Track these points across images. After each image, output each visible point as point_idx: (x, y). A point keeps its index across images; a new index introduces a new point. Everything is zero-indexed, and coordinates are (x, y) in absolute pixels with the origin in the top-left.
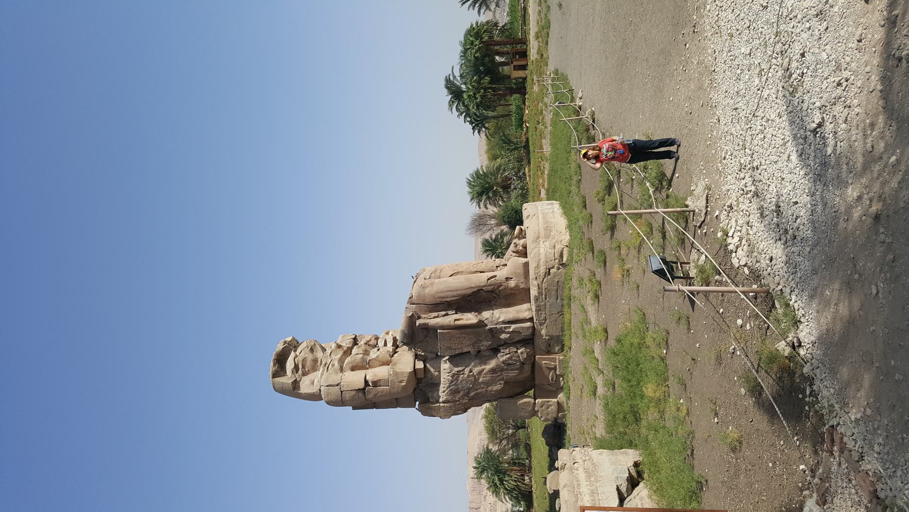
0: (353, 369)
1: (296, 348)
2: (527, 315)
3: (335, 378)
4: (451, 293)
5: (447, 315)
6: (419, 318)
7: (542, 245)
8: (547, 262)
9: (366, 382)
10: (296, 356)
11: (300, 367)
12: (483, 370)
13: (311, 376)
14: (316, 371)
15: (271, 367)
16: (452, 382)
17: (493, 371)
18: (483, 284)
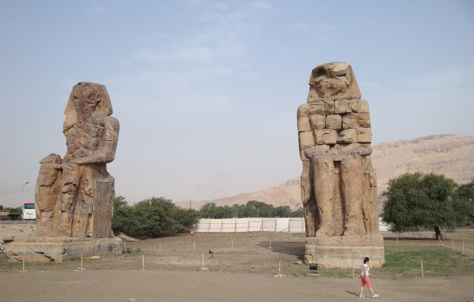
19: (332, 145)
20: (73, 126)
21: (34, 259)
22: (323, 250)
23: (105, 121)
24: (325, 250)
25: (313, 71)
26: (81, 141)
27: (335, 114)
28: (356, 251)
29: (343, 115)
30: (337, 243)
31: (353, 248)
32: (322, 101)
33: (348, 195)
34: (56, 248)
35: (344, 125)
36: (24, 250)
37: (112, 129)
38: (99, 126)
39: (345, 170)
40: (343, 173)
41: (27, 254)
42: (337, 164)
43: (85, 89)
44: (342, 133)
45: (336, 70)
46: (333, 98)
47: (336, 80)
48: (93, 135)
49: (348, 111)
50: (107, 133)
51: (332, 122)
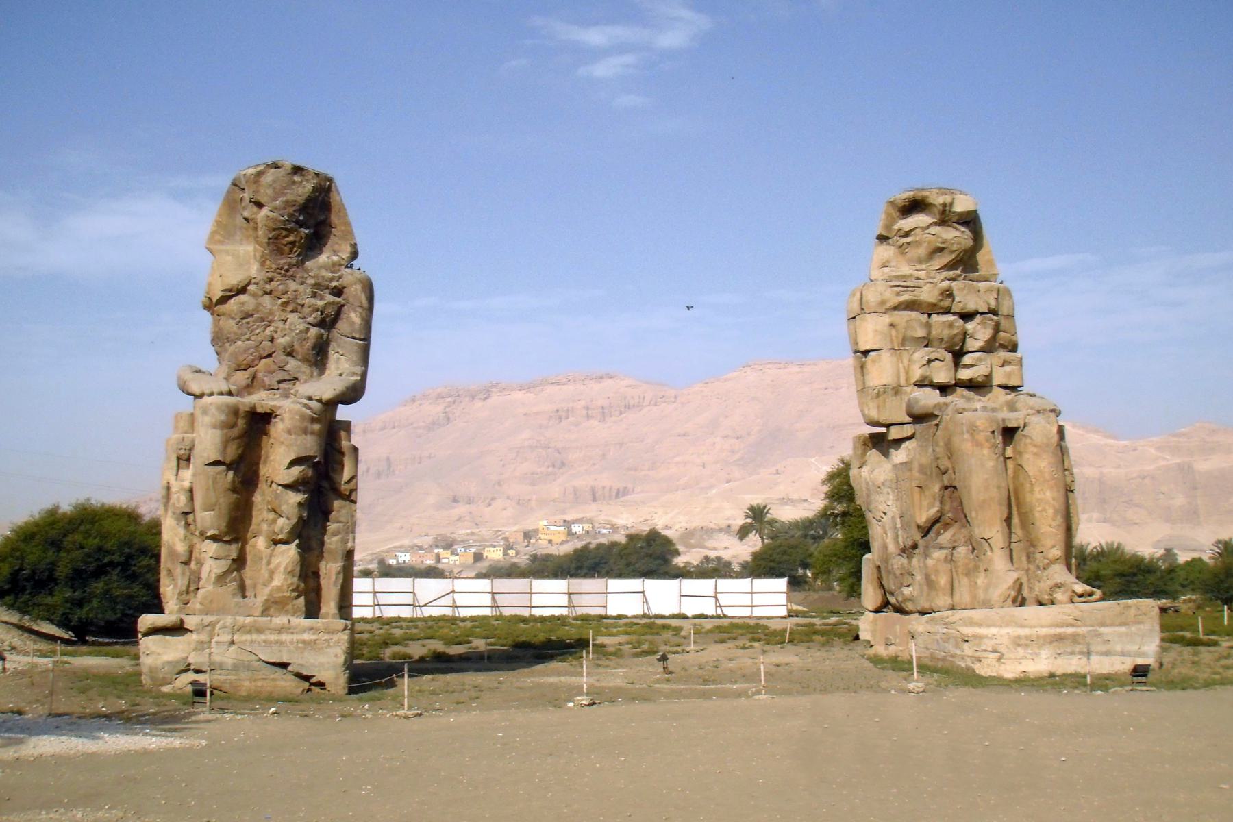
1: (943, 222)
7: (1004, 631)
8: (976, 637)
15: (902, 194)
20: (243, 290)
21: (259, 684)
22: (1038, 637)
23: (344, 282)
26: (275, 336)
27: (948, 311)
28: (1109, 638)
29: (967, 316)
31: (1102, 630)
33: (1044, 510)
34: (332, 651)
35: (972, 344)
36: (227, 657)
37: (365, 303)
38: (330, 298)
39: (1035, 450)
40: (1026, 456)
41: (236, 668)
42: (1009, 433)
43: (294, 182)
44: (967, 359)
48: (309, 319)
50: (353, 315)
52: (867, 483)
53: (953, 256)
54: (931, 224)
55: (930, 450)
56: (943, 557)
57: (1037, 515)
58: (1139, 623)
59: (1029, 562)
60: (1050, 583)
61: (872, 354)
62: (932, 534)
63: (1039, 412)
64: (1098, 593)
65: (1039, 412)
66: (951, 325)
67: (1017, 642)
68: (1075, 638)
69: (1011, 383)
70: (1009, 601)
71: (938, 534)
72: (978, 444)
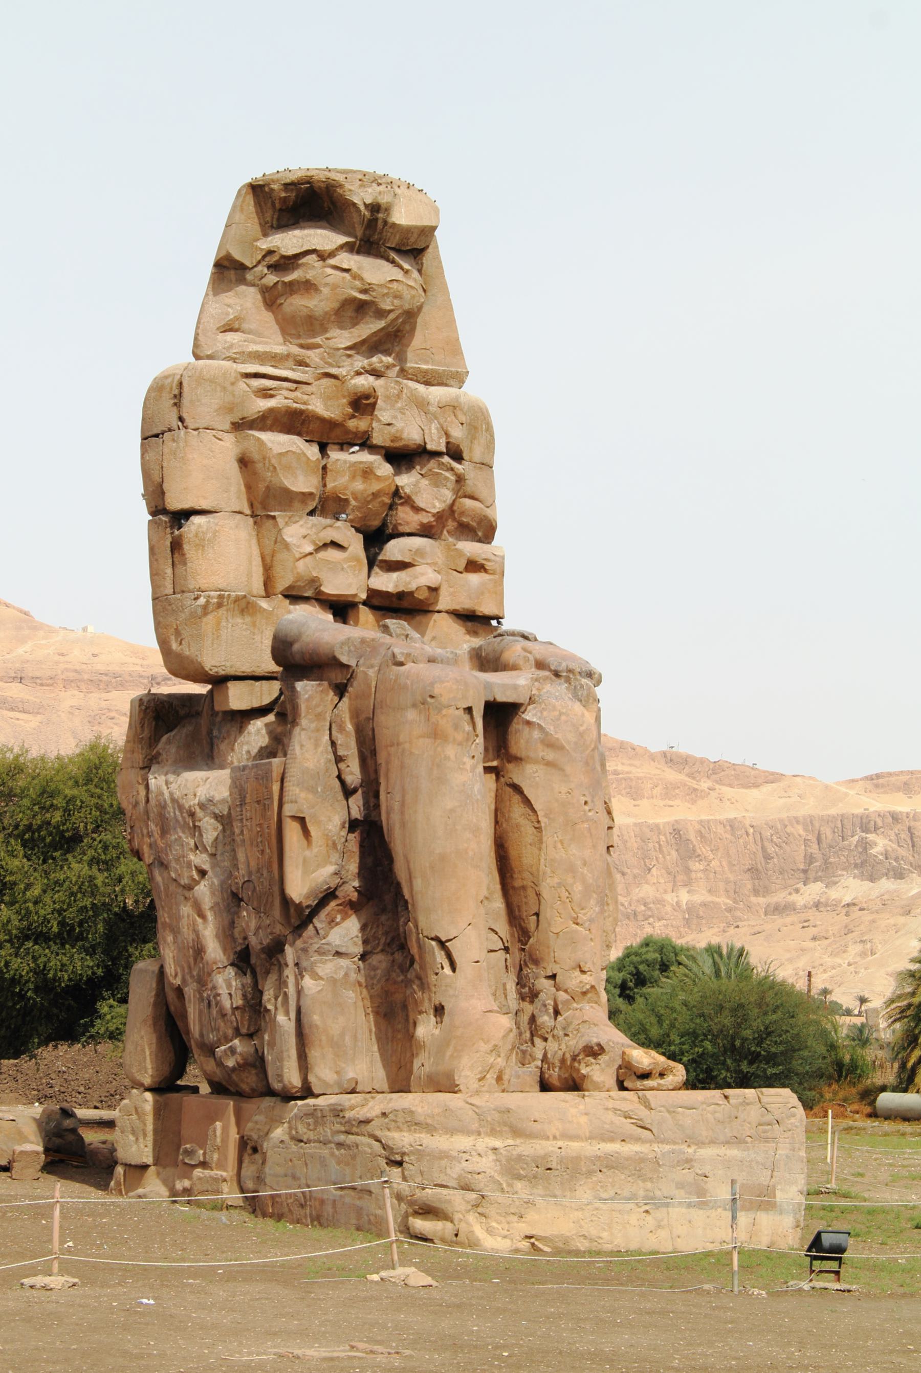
0: (244, 462)
2: (323, 1072)
3: (204, 407)
4: (396, 806)
5: (348, 792)
6: (341, 690)
8: (420, 1154)
9: (182, 516)
10: (323, 256)
11: (288, 279)
12: (202, 916)
13: (261, 319)
14: (284, 332)
16: (181, 808)
17: (199, 951)
18: (422, 923)
19: (341, 609)
24: (577, 1159)
25: (258, 190)
27: (365, 443)
28: (707, 1169)
30: (628, 1127)
32: (302, 363)
35: (406, 517)
39: (550, 755)
40: (530, 769)
44: (394, 549)
45: (402, 216)
46: (360, 362)
47: (396, 274)
49: (430, 446)
51: (359, 486)
52: (163, 807)
53: (381, 324)
54: (342, 247)
55: (328, 737)
56: (341, 974)
57: (546, 893)
58: (766, 1140)
59: (523, 998)
60: (574, 1043)
61: (196, 520)
62: (319, 922)
63: (557, 674)
64: (679, 1072)
65: (557, 674)
66: (367, 473)
67: (514, 1169)
68: (638, 1168)
69: (486, 609)
70: (491, 1077)
71: (332, 923)
72: (436, 734)
